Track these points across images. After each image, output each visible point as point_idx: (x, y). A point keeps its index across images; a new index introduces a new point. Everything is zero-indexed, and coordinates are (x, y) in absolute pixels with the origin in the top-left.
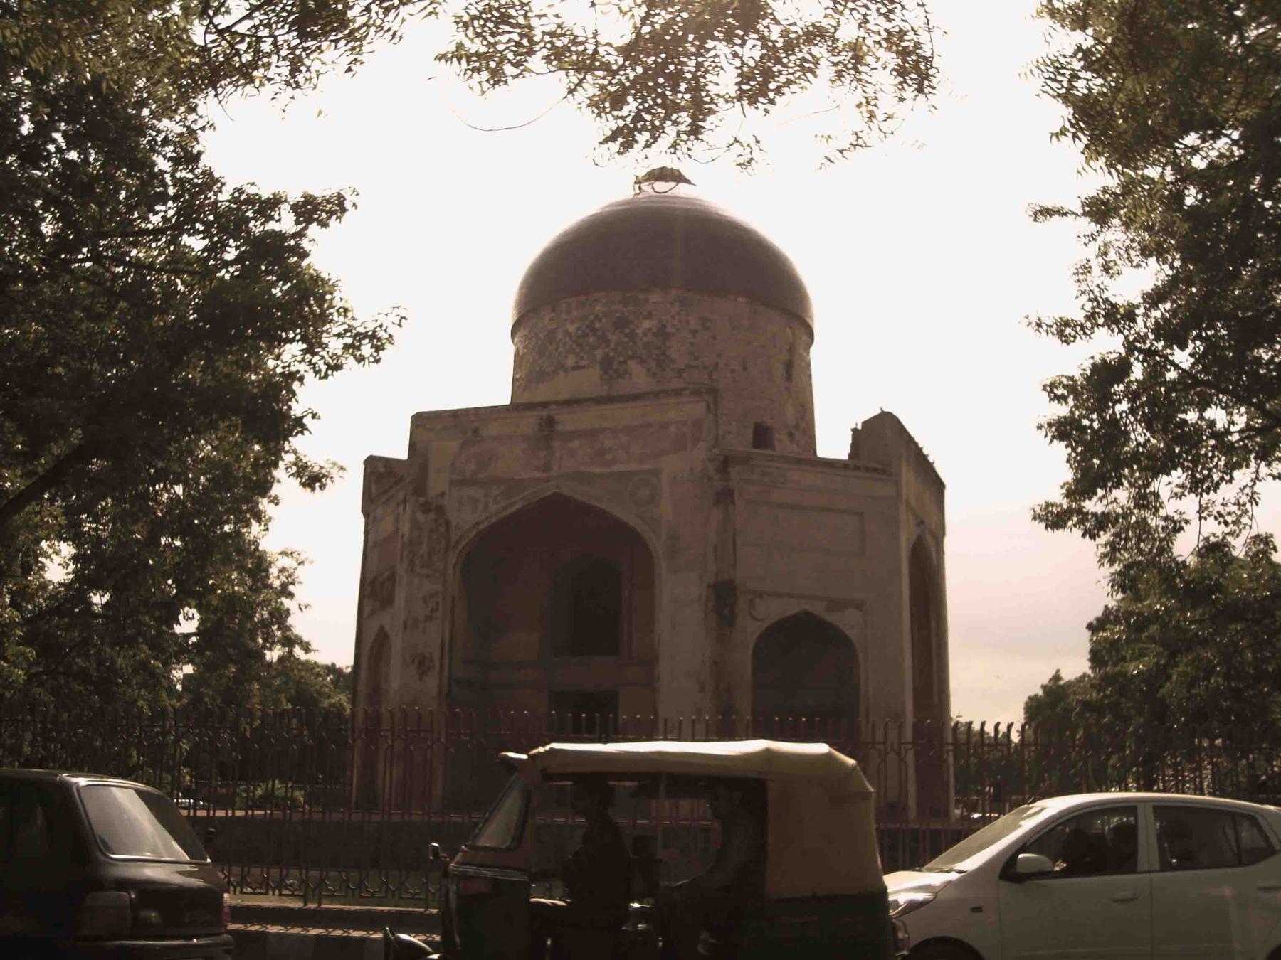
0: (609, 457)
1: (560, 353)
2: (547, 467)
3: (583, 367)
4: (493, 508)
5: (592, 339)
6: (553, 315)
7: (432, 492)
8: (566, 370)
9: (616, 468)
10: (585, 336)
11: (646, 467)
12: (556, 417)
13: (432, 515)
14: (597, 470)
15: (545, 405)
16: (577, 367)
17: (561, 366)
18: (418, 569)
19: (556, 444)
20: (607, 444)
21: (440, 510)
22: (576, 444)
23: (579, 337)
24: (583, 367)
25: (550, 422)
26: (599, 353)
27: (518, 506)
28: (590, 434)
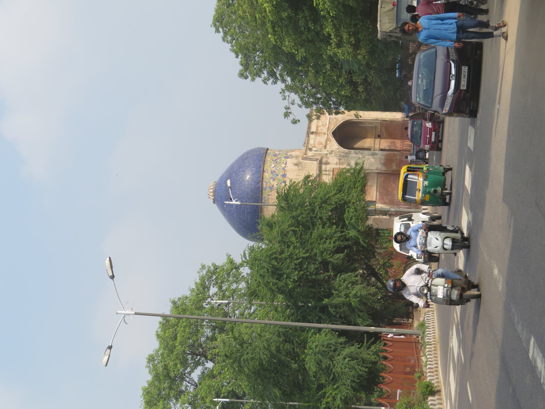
0: (324, 124)
1: (280, 169)
2: (325, 134)
3: (286, 162)
4: (333, 143)
5: (278, 161)
6: (266, 172)
7: (327, 152)
8: (285, 167)
9: (328, 123)
10: (276, 162)
11: (329, 119)
12: (312, 131)
13: (333, 153)
14: (327, 126)
15: (308, 132)
16: (286, 164)
17: (284, 169)
18: (348, 155)
19: (319, 132)
20: (321, 124)
21: (332, 151)
22: (319, 129)
23: (276, 163)
24: (286, 162)
25: (312, 133)
26: (283, 159)
27: (334, 139)
28: (317, 127)
